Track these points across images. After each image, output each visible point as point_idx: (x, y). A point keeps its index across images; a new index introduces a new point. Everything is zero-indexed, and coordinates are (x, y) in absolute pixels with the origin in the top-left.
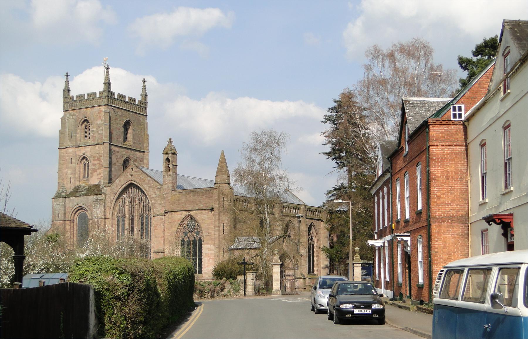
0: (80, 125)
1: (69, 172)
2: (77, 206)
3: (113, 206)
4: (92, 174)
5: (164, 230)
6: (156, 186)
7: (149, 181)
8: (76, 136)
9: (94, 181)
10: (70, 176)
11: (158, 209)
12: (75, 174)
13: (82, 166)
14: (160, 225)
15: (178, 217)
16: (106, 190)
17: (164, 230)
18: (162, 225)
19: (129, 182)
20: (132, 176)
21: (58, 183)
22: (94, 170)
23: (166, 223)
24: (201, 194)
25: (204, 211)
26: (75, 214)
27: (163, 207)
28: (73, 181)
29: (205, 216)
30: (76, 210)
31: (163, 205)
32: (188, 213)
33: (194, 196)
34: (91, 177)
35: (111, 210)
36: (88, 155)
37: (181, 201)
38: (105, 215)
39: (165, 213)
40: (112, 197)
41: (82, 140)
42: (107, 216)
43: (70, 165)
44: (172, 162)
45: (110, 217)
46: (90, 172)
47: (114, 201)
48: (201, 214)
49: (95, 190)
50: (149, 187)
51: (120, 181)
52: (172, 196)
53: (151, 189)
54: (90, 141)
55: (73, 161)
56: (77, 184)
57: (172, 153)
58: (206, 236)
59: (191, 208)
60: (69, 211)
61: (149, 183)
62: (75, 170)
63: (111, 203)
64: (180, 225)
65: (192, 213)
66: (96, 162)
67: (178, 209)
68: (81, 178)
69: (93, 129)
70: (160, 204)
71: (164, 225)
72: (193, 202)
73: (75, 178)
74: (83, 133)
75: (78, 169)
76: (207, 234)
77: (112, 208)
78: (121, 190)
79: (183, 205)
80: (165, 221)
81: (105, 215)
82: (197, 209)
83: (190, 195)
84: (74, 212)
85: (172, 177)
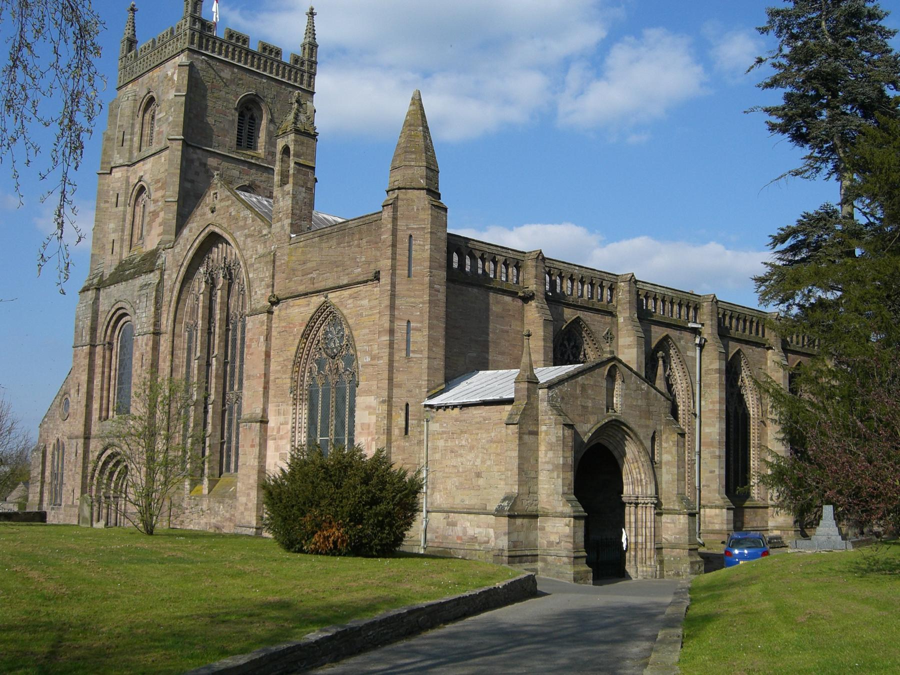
0: (141, 113)
1: (112, 226)
2: (116, 307)
3: (174, 298)
4: (150, 224)
5: (268, 355)
6: (260, 232)
7: (245, 219)
8: (132, 140)
9: (151, 243)
10: (113, 236)
12: (123, 231)
14: (258, 341)
15: (299, 312)
16: (167, 258)
17: (268, 355)
18: (262, 339)
19: (206, 231)
20: (213, 212)
21: (93, 255)
22: (155, 214)
23: (274, 333)
25: (361, 288)
26: (115, 327)
29: (365, 302)
30: (114, 318)
31: (268, 280)
32: (323, 299)
33: (339, 244)
34: (149, 231)
35: (172, 309)
36: (147, 178)
37: (309, 265)
38: (157, 323)
40: (174, 276)
41: (143, 149)
42: (163, 328)
43: (115, 210)
44: (297, 155)
45: (170, 328)
46: (147, 219)
47: (178, 285)
48: (355, 297)
49: (149, 262)
50: (247, 236)
51: (190, 231)
52: (290, 255)
54: (155, 148)
55: (121, 199)
56: (125, 255)
57: (297, 131)
58: (365, 366)
59: (330, 284)
61: (244, 227)
62: (124, 220)
63: (172, 291)
64: (305, 336)
65: (333, 297)
66: (160, 193)
67: (302, 289)
68: (135, 239)
69: (161, 115)
70: (262, 280)
71: (268, 338)
72: (335, 264)
73: (122, 240)
75: (129, 217)
76: (368, 359)
77: (173, 304)
78: (190, 254)
79: (314, 275)
80: (269, 330)
81: (157, 323)
82: (345, 282)
84: (112, 324)
85: (294, 197)
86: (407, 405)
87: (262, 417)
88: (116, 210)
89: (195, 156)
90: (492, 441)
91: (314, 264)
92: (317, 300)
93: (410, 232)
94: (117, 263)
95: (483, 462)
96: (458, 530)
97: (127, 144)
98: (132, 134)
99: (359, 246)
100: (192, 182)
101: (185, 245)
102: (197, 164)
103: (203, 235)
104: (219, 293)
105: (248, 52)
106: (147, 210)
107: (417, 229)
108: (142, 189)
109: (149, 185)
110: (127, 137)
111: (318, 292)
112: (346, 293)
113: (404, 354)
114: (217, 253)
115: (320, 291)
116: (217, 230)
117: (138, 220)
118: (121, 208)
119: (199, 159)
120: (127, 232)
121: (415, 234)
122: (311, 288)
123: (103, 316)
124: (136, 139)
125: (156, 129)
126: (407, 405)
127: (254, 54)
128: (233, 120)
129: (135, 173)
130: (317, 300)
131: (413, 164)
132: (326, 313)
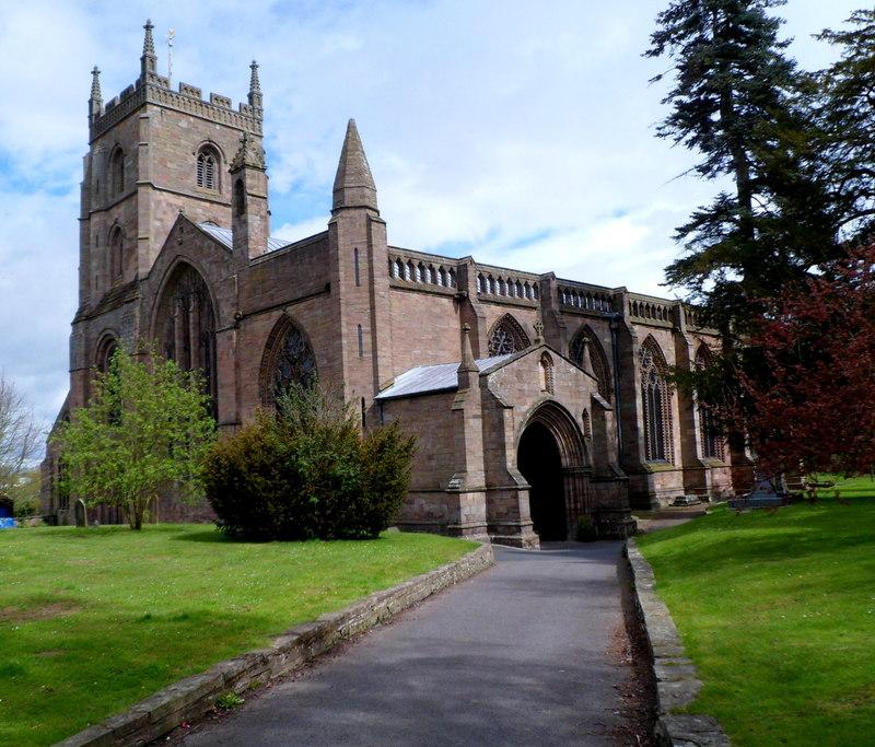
7: (209, 248)
8: (105, 188)
11: (227, 312)
12: (104, 268)
13: (117, 248)
15: (263, 325)
17: (237, 365)
24: (307, 255)
27: (233, 305)
28: (101, 284)
29: (319, 312)
30: (103, 344)
36: (122, 220)
37: (267, 284)
39: (239, 320)
46: (125, 256)
48: (310, 309)
50: (211, 263)
53: (213, 266)
55: (101, 240)
56: (108, 288)
58: (324, 368)
59: (288, 298)
60: (94, 345)
62: (105, 258)
64: (268, 346)
65: (291, 310)
67: (262, 305)
73: (105, 276)
74: (118, 179)
75: (109, 256)
76: (325, 362)
79: (272, 292)
83: (285, 262)
86: (363, 399)
87: (237, 419)
88: (97, 250)
89: (162, 197)
90: (440, 427)
91: (272, 282)
92: (277, 314)
93: (354, 246)
94: (102, 295)
95: (433, 446)
96: (416, 507)
97: (102, 191)
98: (106, 182)
99: (310, 263)
100: (161, 220)
101: (159, 275)
102: (164, 204)
103: (174, 265)
104: (191, 315)
105: (202, 103)
106: (124, 247)
107: (360, 243)
108: (118, 230)
109: (124, 226)
110: (102, 185)
111: (277, 307)
112: (302, 306)
113: (357, 355)
114: (185, 281)
115: (277, 306)
116: (185, 260)
117: (117, 257)
118: (101, 248)
119: (166, 200)
120: (108, 268)
121: (359, 247)
122: (270, 303)
123: (93, 342)
124: (109, 186)
125: (126, 176)
126: (363, 399)
127: (207, 105)
128: (193, 166)
129: (111, 216)
130: (277, 314)
131: (353, 185)
132: (288, 328)
